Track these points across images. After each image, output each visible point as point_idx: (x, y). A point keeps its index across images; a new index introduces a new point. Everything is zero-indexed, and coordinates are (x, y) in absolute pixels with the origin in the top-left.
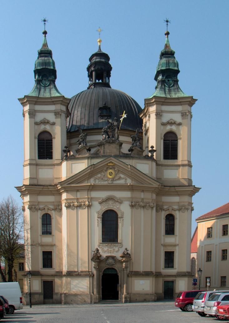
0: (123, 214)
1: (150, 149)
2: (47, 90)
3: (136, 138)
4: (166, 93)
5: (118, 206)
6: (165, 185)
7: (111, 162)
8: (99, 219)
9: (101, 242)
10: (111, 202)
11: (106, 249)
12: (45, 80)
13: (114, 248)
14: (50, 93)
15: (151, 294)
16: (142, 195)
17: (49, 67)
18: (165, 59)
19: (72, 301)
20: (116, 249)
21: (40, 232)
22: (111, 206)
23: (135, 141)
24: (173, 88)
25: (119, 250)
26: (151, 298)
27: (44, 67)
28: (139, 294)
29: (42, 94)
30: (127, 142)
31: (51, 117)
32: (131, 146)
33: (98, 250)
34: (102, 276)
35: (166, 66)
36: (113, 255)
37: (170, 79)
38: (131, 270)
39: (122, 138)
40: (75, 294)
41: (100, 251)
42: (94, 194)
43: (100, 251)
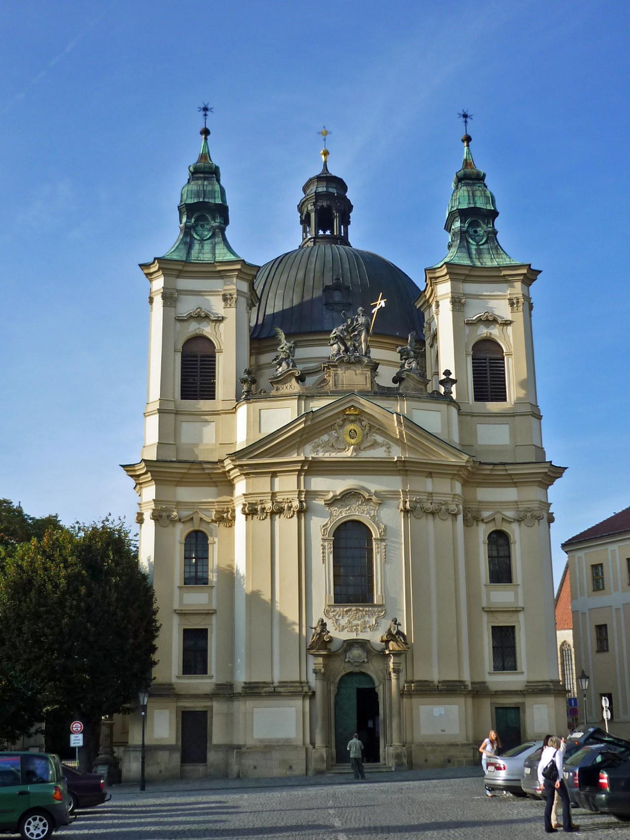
1: (443, 377)
2: (207, 247)
3: (408, 354)
4: (474, 256)
6: (482, 461)
7: (353, 406)
9: (333, 603)
11: (344, 621)
14: (214, 254)
15: (463, 745)
16: (428, 485)
17: (212, 201)
18: (464, 188)
19: (255, 767)
23: (406, 359)
24: (485, 246)
26: (465, 757)
27: (201, 200)
28: (433, 745)
29: (196, 255)
30: (389, 363)
32: (398, 370)
33: (323, 625)
36: (362, 636)
38: (409, 679)
39: (376, 354)
40: (265, 747)
41: (328, 628)
43: (330, 627)
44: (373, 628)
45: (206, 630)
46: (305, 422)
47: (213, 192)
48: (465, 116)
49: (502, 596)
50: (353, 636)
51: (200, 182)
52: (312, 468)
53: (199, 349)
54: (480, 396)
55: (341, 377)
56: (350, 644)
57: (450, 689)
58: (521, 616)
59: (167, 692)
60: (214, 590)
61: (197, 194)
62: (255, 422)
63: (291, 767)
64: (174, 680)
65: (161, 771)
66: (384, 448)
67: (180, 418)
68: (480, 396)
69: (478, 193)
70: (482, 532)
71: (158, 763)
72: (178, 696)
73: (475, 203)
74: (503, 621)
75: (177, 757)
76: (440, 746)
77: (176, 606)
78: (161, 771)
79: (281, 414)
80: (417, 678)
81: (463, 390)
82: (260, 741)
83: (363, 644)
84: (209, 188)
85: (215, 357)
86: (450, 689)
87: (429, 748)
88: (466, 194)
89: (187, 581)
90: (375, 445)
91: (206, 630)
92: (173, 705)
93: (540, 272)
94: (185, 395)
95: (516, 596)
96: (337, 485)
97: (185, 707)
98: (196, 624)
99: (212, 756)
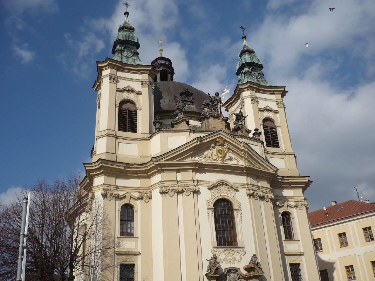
5: (233, 195)
9: (216, 245)
10: (223, 188)
20: (238, 257)
22: (223, 193)
31: (137, 87)
44: (239, 261)
46: (197, 142)
48: (243, 28)
52: (200, 168)
53: (127, 106)
56: (229, 271)
60: (139, 240)
62: (164, 143)
66: (236, 161)
67: (118, 140)
79: (178, 139)
83: (236, 270)
84: (131, 35)
85: (136, 112)
90: (230, 159)
93: (288, 92)
94: (121, 129)
95: (299, 246)
96: (213, 177)
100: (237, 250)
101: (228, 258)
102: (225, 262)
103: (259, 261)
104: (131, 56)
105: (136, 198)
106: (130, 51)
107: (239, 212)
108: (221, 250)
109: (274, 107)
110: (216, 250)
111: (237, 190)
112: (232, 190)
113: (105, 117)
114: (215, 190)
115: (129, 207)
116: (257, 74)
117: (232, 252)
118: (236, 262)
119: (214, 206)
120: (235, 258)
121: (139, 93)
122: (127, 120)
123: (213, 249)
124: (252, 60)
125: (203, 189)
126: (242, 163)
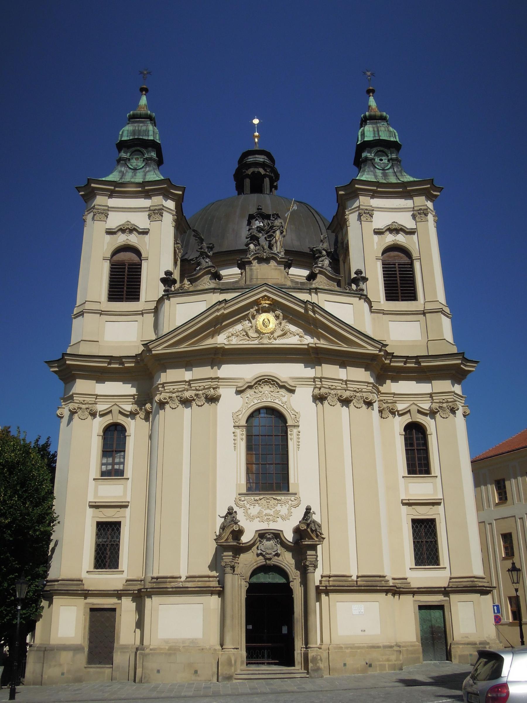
0: (296, 415)
1: (353, 276)
5: (284, 399)
7: (265, 296)
8: (238, 431)
9: (244, 491)
10: (266, 389)
11: (254, 510)
12: (137, 159)
13: (279, 507)
15: (385, 647)
16: (342, 373)
17: (146, 138)
19: (158, 671)
20: (283, 510)
21: (94, 470)
22: (268, 397)
24: (391, 171)
25: (290, 514)
26: (388, 660)
27: (136, 137)
28: (352, 647)
31: (141, 220)
34: (248, 591)
35: (375, 136)
36: (273, 526)
37: (383, 158)
38: (327, 573)
40: (170, 649)
41: (239, 517)
42: (228, 370)
43: (240, 516)
45: (119, 524)
47: (147, 131)
49: (421, 488)
50: (264, 526)
51: (136, 125)
54: (391, 296)
55: (255, 273)
57: (371, 586)
58: (441, 508)
59: (75, 590)
61: (134, 132)
63: (196, 672)
64: (84, 575)
65: (63, 674)
68: (391, 296)
69: (383, 129)
70: (398, 424)
71: (60, 665)
72: (86, 594)
73: (379, 136)
74: (423, 513)
75: (82, 658)
76: (359, 648)
77: (91, 498)
78: (63, 674)
80: (333, 573)
81: (376, 286)
82: (166, 641)
83: (277, 536)
84: (144, 128)
86: (371, 586)
87: (348, 651)
88: (371, 129)
89: (103, 474)
91: (119, 524)
92: (81, 602)
97: (93, 604)
98: (109, 516)
99: (119, 658)
100: (283, 498)
101: (268, 511)
102: (258, 519)
103: (316, 517)
104: (141, 167)
105: (129, 413)
106: (141, 158)
107: (295, 431)
108: (252, 498)
109: (408, 222)
110: (243, 499)
111: (292, 391)
112: (283, 392)
113: (94, 279)
114: (250, 393)
115: (119, 428)
116: (386, 161)
117: (273, 502)
118: (279, 520)
119: (247, 422)
120: (277, 512)
121: (145, 232)
122: (124, 282)
123: (239, 496)
124: (377, 135)
125: (227, 394)
126: (309, 340)
